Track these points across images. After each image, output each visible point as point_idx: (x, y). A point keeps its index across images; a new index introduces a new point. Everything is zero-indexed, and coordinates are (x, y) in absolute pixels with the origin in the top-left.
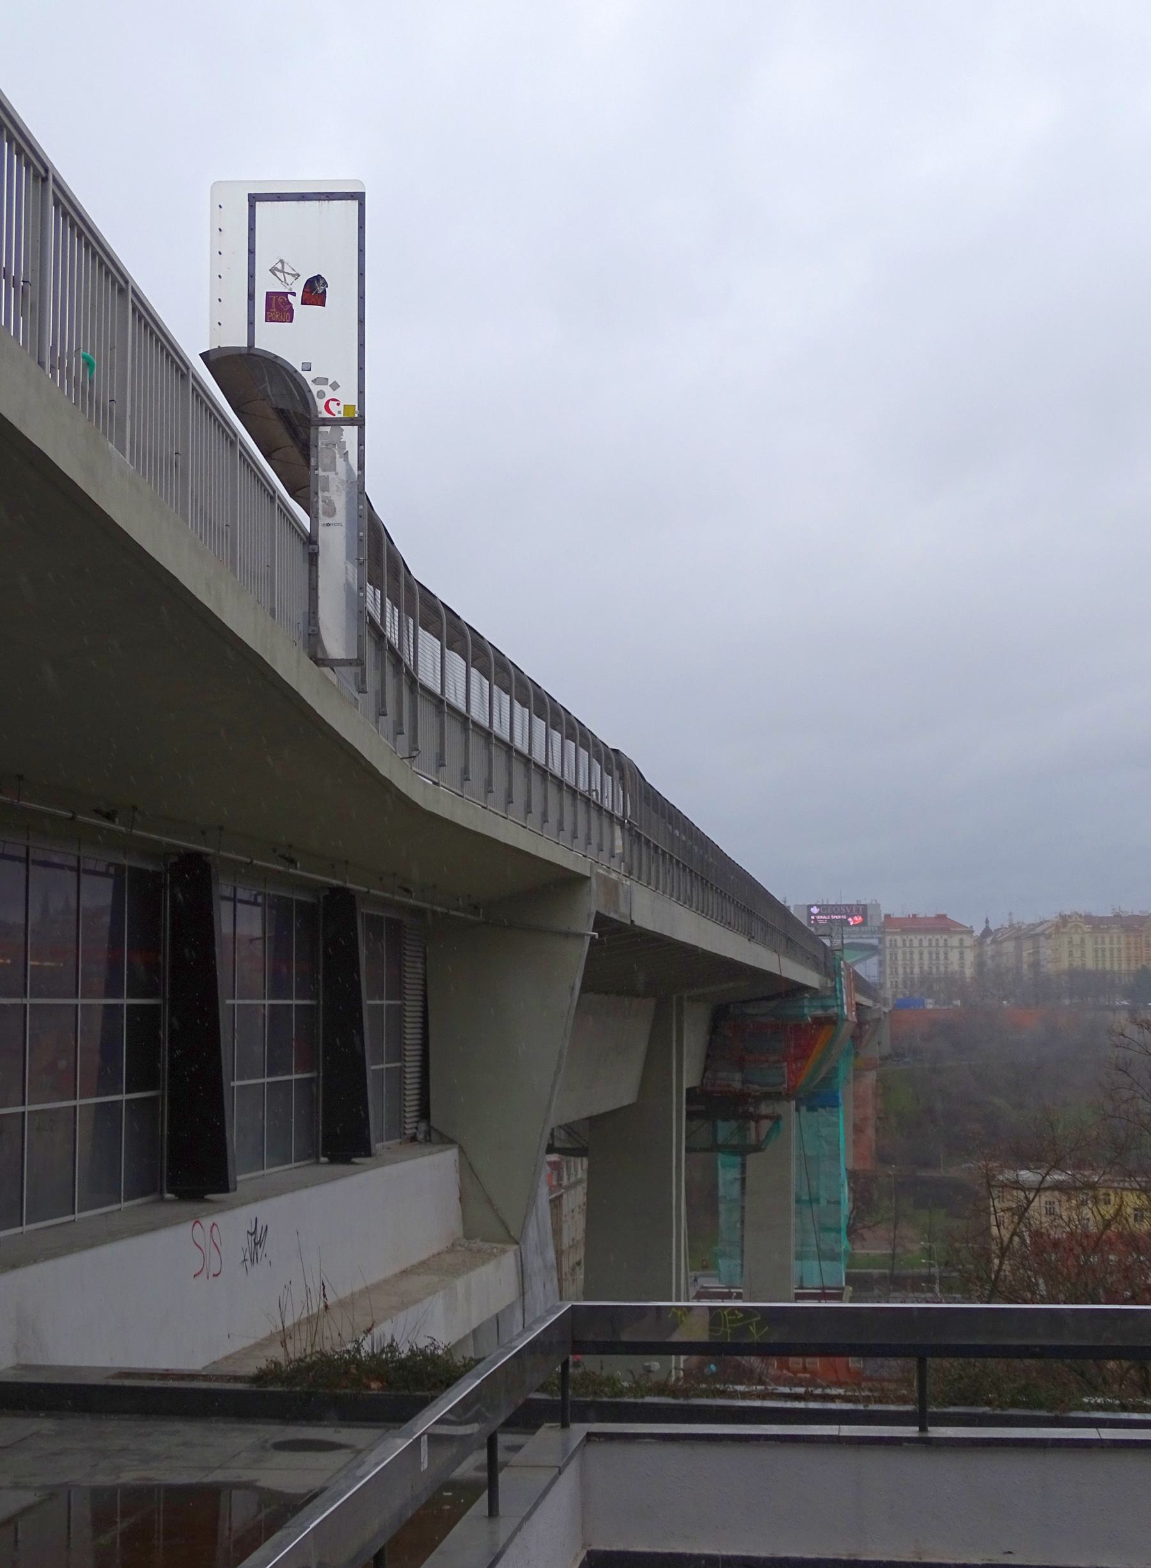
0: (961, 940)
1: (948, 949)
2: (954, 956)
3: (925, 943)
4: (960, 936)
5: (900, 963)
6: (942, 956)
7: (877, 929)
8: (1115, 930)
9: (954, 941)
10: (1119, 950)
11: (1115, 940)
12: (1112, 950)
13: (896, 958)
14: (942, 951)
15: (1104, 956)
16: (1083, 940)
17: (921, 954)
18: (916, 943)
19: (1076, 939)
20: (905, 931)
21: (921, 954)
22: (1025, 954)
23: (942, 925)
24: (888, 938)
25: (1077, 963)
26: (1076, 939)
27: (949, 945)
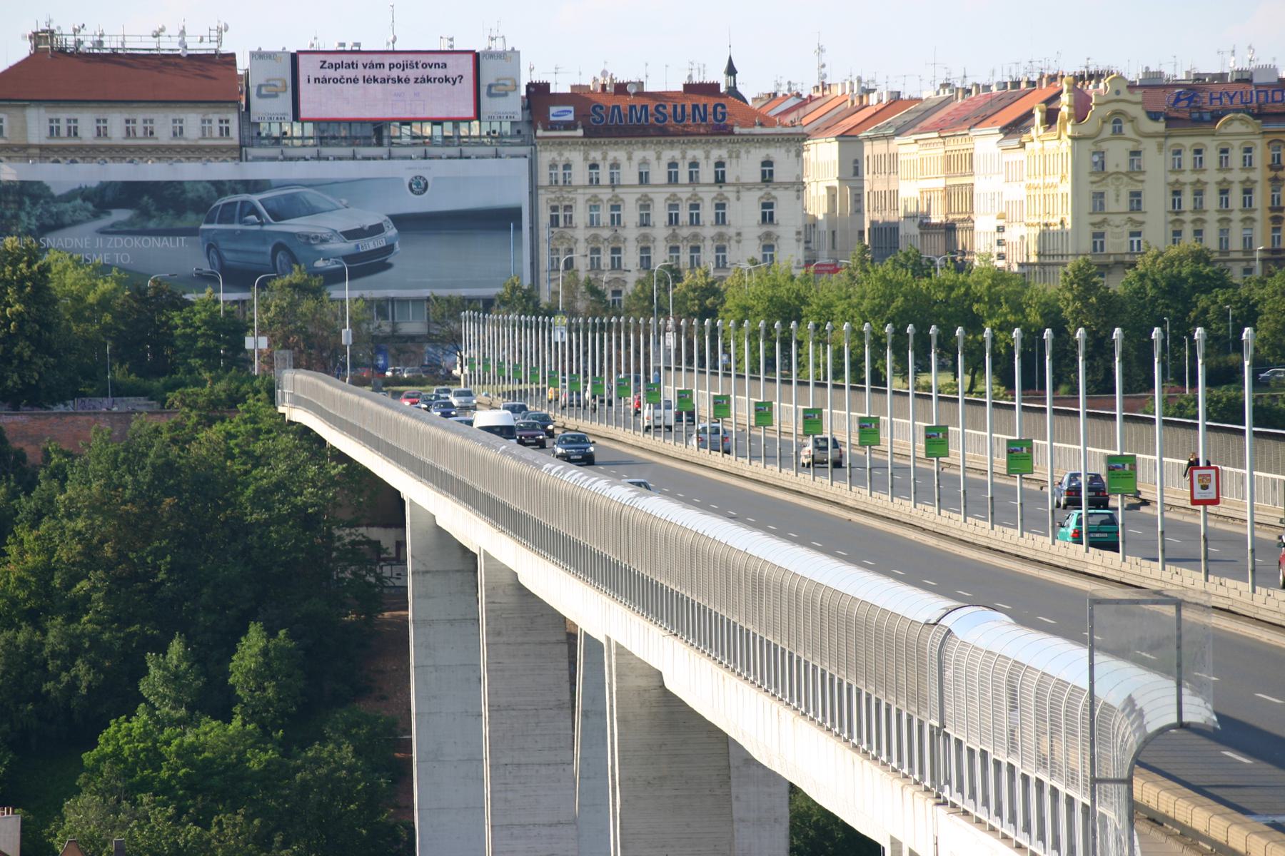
0: (767, 163)
1: (729, 192)
5: (581, 233)
6: (708, 214)
7: (507, 127)
8: (1237, 127)
9: (746, 166)
11: (1236, 157)
13: (569, 219)
14: (708, 197)
15: (1198, 208)
17: (645, 205)
18: (629, 174)
21: (645, 205)
27: (728, 179)
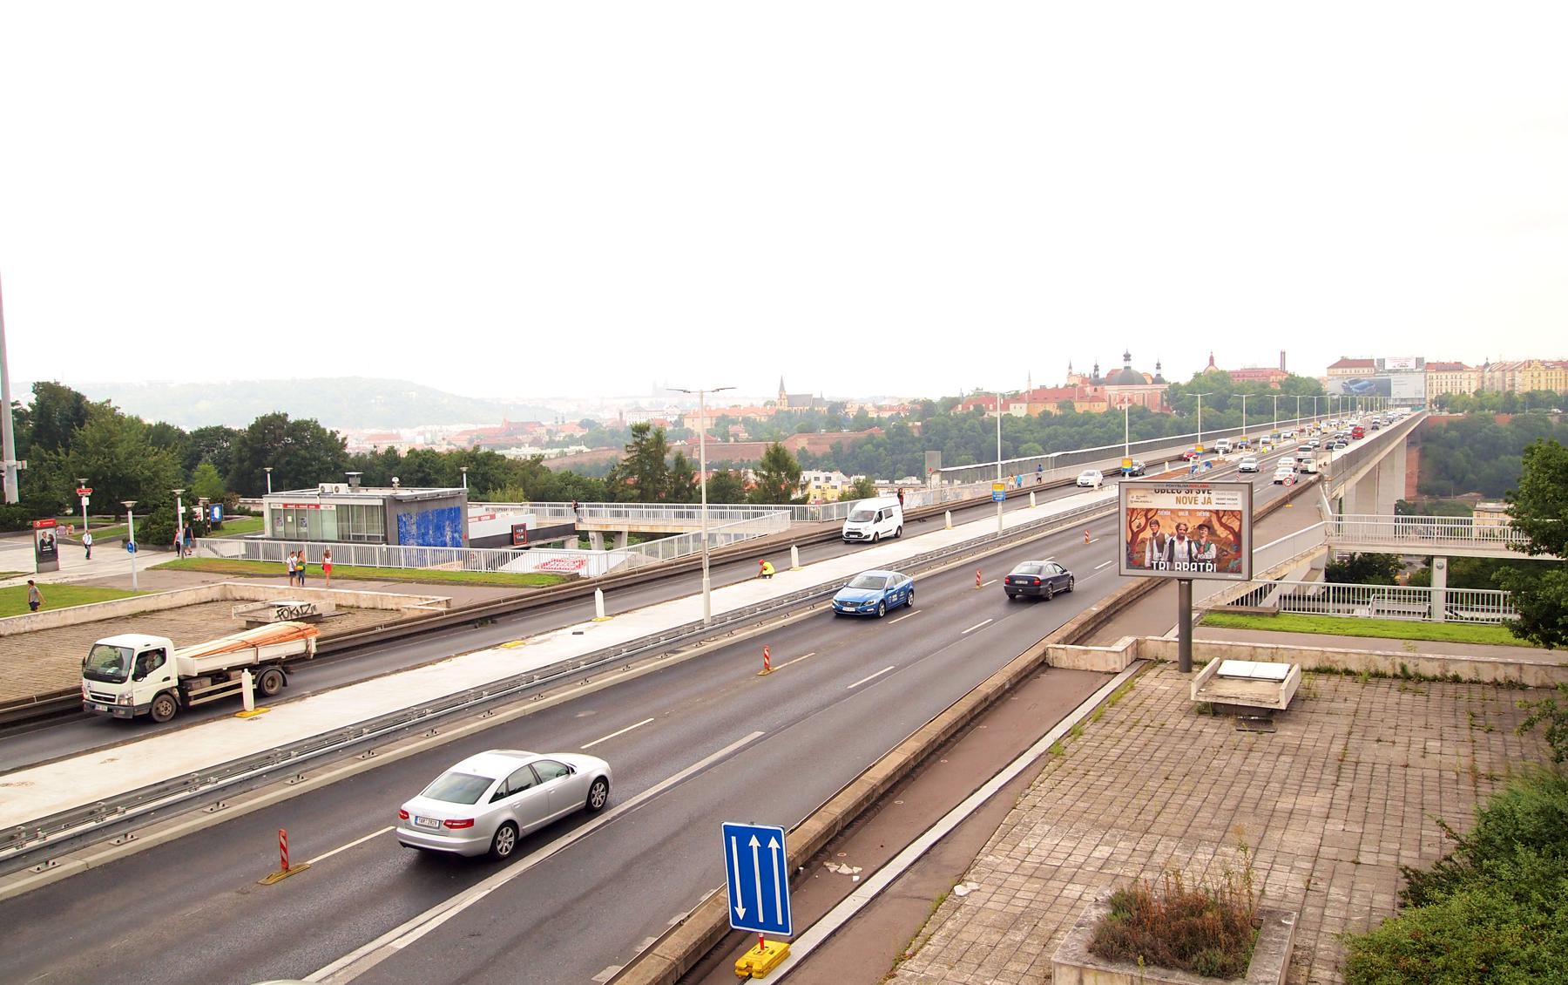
2: (1465, 384)
3: (1449, 377)
4: (1468, 374)
5: (1435, 387)
6: (1458, 384)
9: (1466, 375)
10: (1561, 379)
11: (1558, 374)
12: (1556, 380)
15: (1551, 382)
16: (1539, 375)
18: (1444, 377)
19: (1536, 374)
20: (1437, 371)
22: (1507, 380)
23: (1458, 367)
24: (1428, 375)
25: (1536, 388)
26: (1536, 374)
